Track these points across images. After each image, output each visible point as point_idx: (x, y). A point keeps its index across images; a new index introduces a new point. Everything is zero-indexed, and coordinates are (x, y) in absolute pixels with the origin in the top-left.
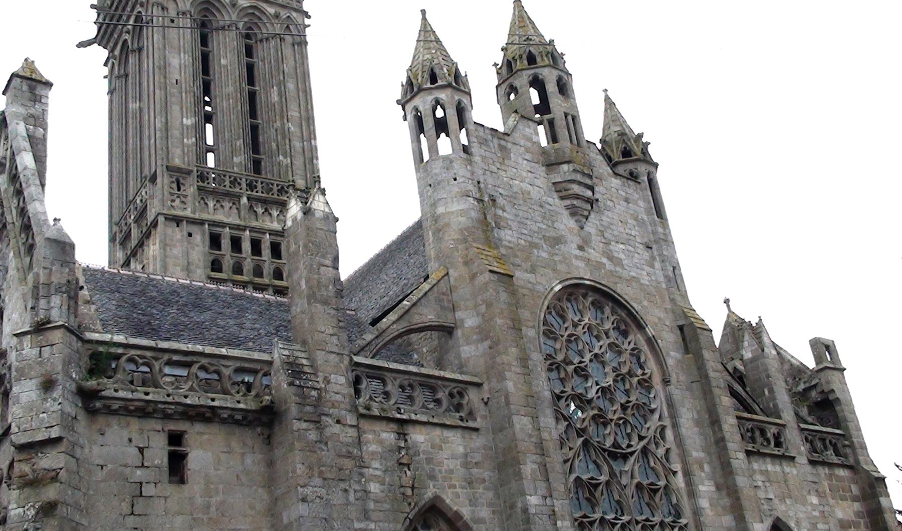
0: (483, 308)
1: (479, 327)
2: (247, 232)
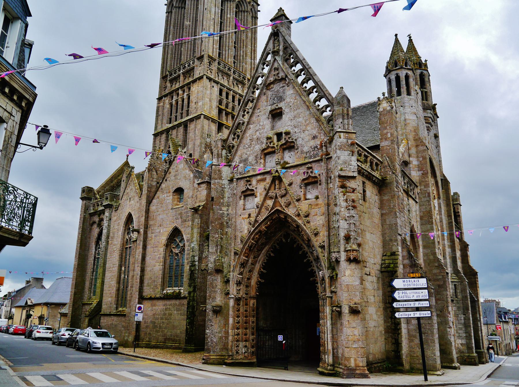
0: (421, 159)
1: (418, 165)
2: (232, 92)
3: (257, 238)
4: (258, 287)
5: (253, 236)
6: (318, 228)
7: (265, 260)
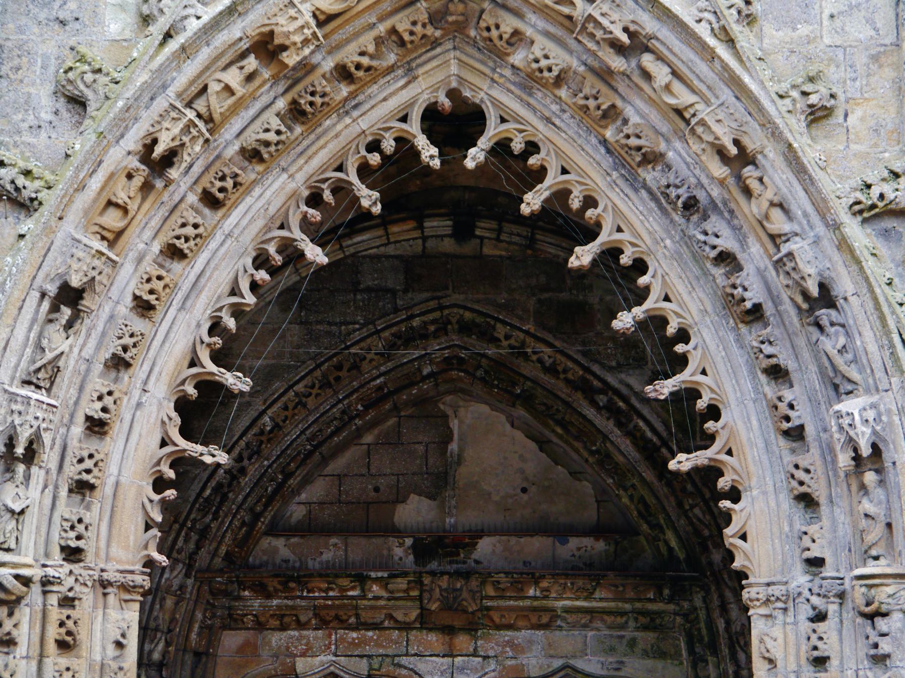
3: (228, 90)
4: (165, 506)
5: (191, 69)
6: (833, 74)
7: (245, 286)
